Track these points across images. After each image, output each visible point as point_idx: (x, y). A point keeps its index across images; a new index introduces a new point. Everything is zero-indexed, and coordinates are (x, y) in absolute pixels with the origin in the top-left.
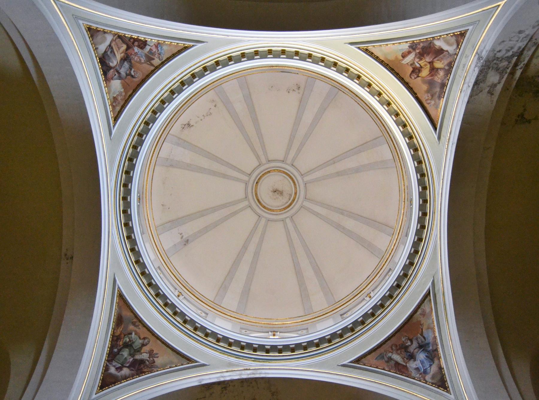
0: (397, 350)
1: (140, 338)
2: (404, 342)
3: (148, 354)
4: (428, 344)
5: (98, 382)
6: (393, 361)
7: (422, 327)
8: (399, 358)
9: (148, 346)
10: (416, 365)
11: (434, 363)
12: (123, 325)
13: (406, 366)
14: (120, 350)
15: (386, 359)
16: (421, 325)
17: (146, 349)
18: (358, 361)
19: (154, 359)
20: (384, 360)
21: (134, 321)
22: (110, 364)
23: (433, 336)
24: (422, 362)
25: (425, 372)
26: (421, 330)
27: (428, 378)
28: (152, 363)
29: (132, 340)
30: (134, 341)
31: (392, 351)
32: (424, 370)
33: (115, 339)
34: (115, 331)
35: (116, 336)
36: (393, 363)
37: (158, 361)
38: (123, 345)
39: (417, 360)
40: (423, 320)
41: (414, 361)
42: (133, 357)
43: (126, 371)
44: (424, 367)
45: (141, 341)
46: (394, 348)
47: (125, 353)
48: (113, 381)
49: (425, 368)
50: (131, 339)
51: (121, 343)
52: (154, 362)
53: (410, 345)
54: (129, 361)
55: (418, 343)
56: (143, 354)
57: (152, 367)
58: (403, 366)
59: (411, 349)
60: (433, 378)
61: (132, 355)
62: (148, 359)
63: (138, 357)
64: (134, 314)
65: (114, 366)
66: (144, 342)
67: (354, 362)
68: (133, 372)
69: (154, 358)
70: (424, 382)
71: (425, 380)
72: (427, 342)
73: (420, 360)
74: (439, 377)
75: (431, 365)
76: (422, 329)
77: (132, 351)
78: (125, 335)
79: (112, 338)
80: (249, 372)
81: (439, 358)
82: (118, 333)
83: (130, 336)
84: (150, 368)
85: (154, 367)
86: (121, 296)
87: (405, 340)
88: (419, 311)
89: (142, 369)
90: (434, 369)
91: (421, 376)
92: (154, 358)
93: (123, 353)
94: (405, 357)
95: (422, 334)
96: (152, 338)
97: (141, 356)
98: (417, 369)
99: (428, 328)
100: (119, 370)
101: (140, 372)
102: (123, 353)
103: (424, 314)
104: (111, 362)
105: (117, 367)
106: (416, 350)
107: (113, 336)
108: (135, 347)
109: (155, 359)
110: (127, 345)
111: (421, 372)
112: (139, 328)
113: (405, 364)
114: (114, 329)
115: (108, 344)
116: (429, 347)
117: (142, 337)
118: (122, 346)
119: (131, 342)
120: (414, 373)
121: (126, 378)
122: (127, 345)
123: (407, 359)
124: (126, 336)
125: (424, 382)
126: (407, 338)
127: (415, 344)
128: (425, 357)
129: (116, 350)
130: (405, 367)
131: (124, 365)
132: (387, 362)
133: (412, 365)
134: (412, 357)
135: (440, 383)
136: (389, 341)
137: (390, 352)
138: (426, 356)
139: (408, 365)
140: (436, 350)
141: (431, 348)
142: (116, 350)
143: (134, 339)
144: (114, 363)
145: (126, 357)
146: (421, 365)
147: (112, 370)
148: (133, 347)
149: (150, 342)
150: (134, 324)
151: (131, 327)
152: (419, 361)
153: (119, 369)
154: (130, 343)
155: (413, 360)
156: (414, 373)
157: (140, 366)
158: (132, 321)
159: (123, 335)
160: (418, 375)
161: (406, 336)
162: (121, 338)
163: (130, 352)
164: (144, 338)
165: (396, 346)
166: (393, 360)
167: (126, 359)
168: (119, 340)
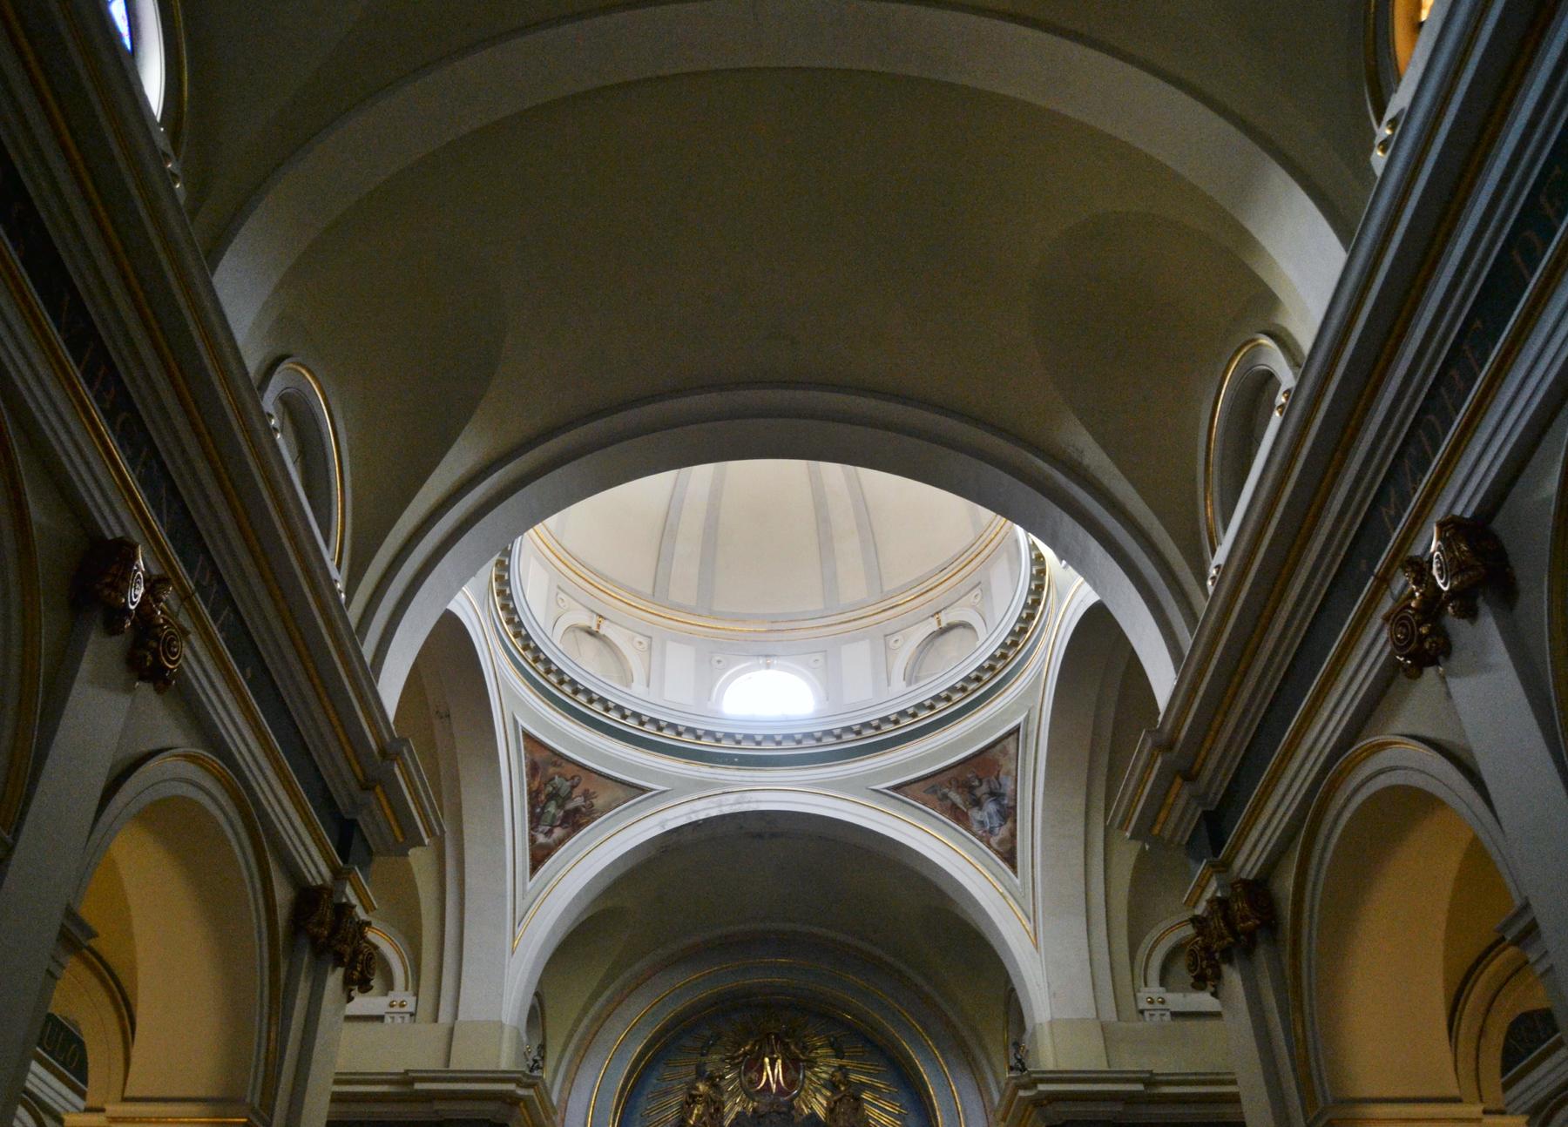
0: (958, 787)
1: (567, 780)
9: (580, 785)
14: (543, 808)
15: (939, 794)
17: (577, 791)
18: (896, 788)
24: (990, 816)
27: (994, 841)
33: (534, 796)
36: (948, 803)
37: (598, 802)
40: (1002, 761)
43: (558, 832)
45: (568, 783)
46: (953, 783)
47: (552, 808)
48: (546, 852)
51: (543, 797)
60: (1001, 843)
61: (559, 807)
63: (570, 806)
65: (542, 832)
72: (1002, 791)
73: (988, 814)
74: (1009, 846)
75: (1001, 825)
78: (545, 784)
80: (732, 798)
81: (1015, 821)
82: (535, 785)
86: (528, 737)
88: (999, 747)
90: (1003, 832)
96: (582, 773)
98: (982, 823)
99: (1008, 773)
101: (577, 827)
103: (1005, 752)
106: (985, 796)
107: (530, 793)
109: (594, 801)
110: (551, 797)
114: (529, 785)
120: (975, 827)
121: (561, 842)
122: (551, 797)
127: (984, 788)
129: (538, 810)
130: (965, 814)
132: (940, 800)
133: (975, 814)
134: (977, 803)
135: (1006, 856)
139: (969, 813)
140: (1014, 808)
141: (1006, 802)
142: (538, 810)
144: (540, 829)
147: (541, 839)
150: (555, 764)
151: (551, 770)
152: (986, 814)
153: (548, 833)
156: (975, 827)
164: (573, 778)
165: (958, 782)
167: (554, 815)
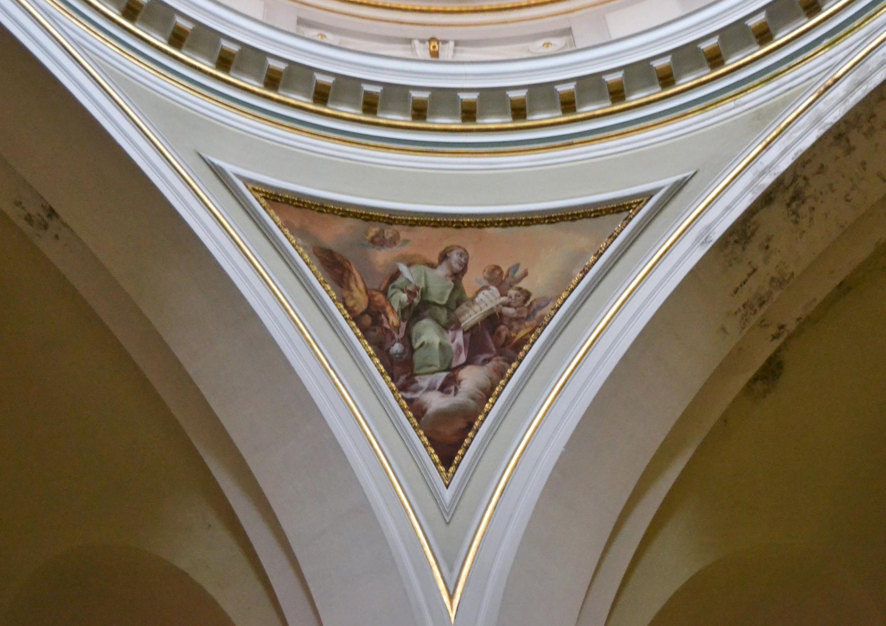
1: (432, 266)
3: (494, 289)
5: (428, 457)
12: (355, 271)
19: (520, 289)
21: (371, 234)
22: (415, 391)
28: (525, 301)
29: (417, 288)
30: (422, 285)
34: (350, 303)
35: (363, 313)
38: (403, 319)
42: (458, 326)
45: (442, 271)
48: (461, 424)
50: (410, 288)
51: (394, 319)
52: (528, 295)
54: (459, 348)
56: (477, 300)
57: (534, 312)
61: (450, 325)
62: (504, 299)
63: (471, 316)
64: (356, 216)
65: (430, 389)
66: (450, 266)
68: (490, 365)
69: (521, 285)
77: (443, 315)
78: (385, 292)
79: (359, 325)
82: (360, 300)
83: (399, 282)
84: (528, 318)
85: (540, 308)
89: (508, 339)
92: (521, 285)
93: (424, 338)
97: (476, 308)
100: (452, 388)
102: (424, 338)
104: (413, 387)
105: (438, 385)
107: (355, 318)
108: (442, 299)
112: (406, 241)
115: (363, 349)
117: (435, 260)
118: (403, 325)
119: (418, 294)
121: (488, 393)
124: (391, 292)
129: (397, 348)
131: (454, 365)
142: (397, 348)
143: (419, 280)
144: (424, 382)
145: (440, 344)
147: (436, 402)
148: (436, 304)
149: (470, 251)
150: (379, 242)
151: (382, 257)
154: (416, 301)
157: (499, 334)
158: (368, 238)
159: (379, 297)
162: (383, 308)
163: (437, 321)
168: (383, 316)
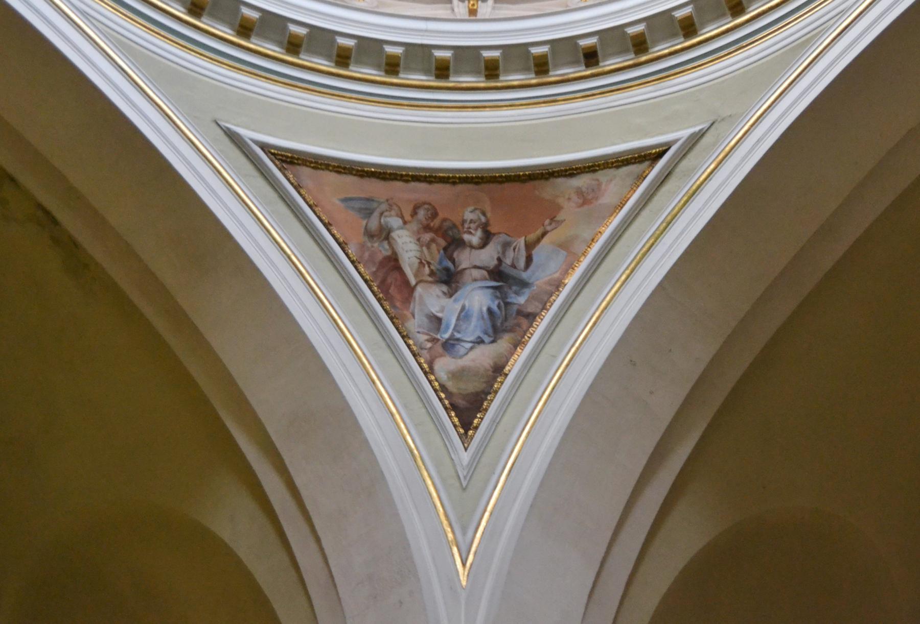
2: (464, 222)
4: (524, 284)
6: (387, 247)
7: (548, 228)
8: (412, 254)
10: (442, 311)
11: (493, 342)
13: (412, 290)
15: (374, 224)
16: (552, 219)
20: (364, 222)
23: (557, 275)
24: (464, 315)
25: (449, 346)
26: (539, 232)
27: (445, 365)
31: (408, 217)
32: (452, 338)
36: (384, 250)
39: (455, 301)
41: (444, 293)
44: (459, 332)
49: (458, 335)
53: (472, 247)
55: (499, 260)
58: (406, 282)
59: (465, 259)
60: (458, 375)
67: (273, 154)
70: (425, 366)
71: (431, 364)
72: (525, 275)
73: (463, 308)
75: (480, 341)
76: (544, 234)
81: (518, 344)
87: (471, 221)
88: (582, 181)
91: (429, 345)
94: (429, 263)
95: (530, 247)
98: (437, 321)
99: (565, 245)
103: (585, 198)
106: (476, 273)
111: (438, 337)
113: (413, 281)
116: (517, 293)
123: (432, 273)
125: (425, 366)
126: (483, 219)
127: (488, 256)
128: (485, 309)
130: (408, 290)
136: (423, 186)
137: (402, 217)
138: (490, 311)
139: (419, 289)
140: (531, 317)
141: (521, 300)
146: (453, 321)
152: (458, 307)
155: (445, 288)
160: (426, 337)
161: (484, 214)
166: (390, 244)
